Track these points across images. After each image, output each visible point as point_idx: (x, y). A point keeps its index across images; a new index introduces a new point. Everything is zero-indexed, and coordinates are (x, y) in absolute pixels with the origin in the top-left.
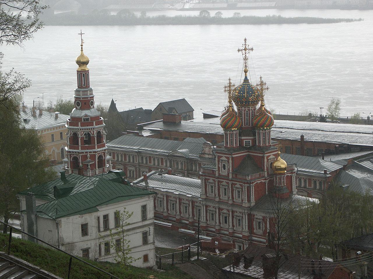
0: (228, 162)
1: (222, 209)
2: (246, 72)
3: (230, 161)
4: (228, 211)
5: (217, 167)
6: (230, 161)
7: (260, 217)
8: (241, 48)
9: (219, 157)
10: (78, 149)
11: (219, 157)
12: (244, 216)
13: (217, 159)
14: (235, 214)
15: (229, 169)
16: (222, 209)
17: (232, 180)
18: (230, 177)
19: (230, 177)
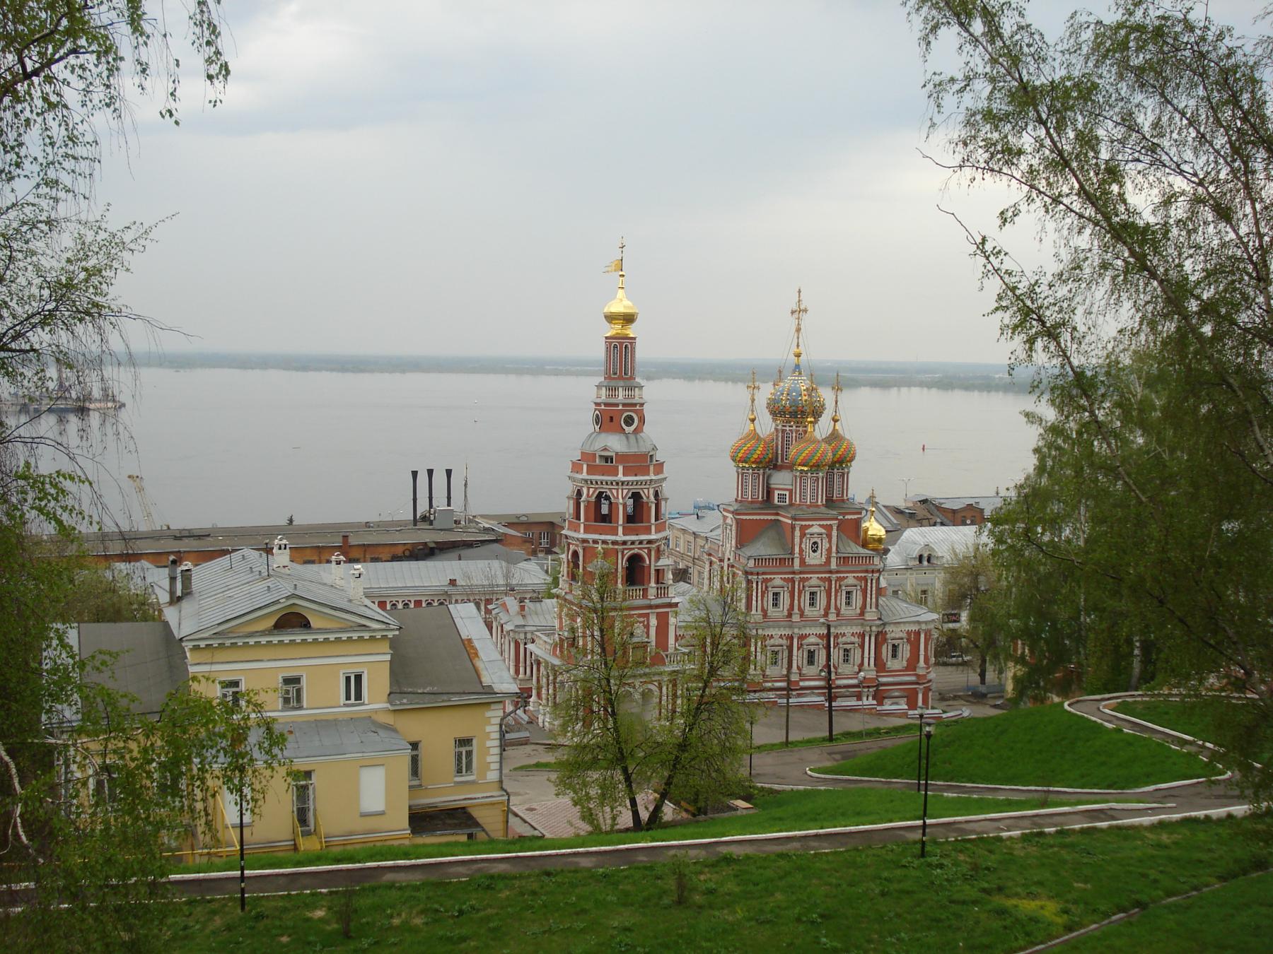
0: (829, 536)
1: (806, 636)
2: (798, 355)
3: (834, 533)
4: (820, 636)
5: (797, 550)
6: (834, 533)
7: (901, 635)
8: (795, 308)
9: (803, 528)
10: (650, 533)
11: (803, 528)
12: (867, 639)
13: (797, 533)
14: (841, 640)
15: (829, 550)
16: (806, 636)
17: (838, 572)
18: (833, 566)
19: (833, 566)
